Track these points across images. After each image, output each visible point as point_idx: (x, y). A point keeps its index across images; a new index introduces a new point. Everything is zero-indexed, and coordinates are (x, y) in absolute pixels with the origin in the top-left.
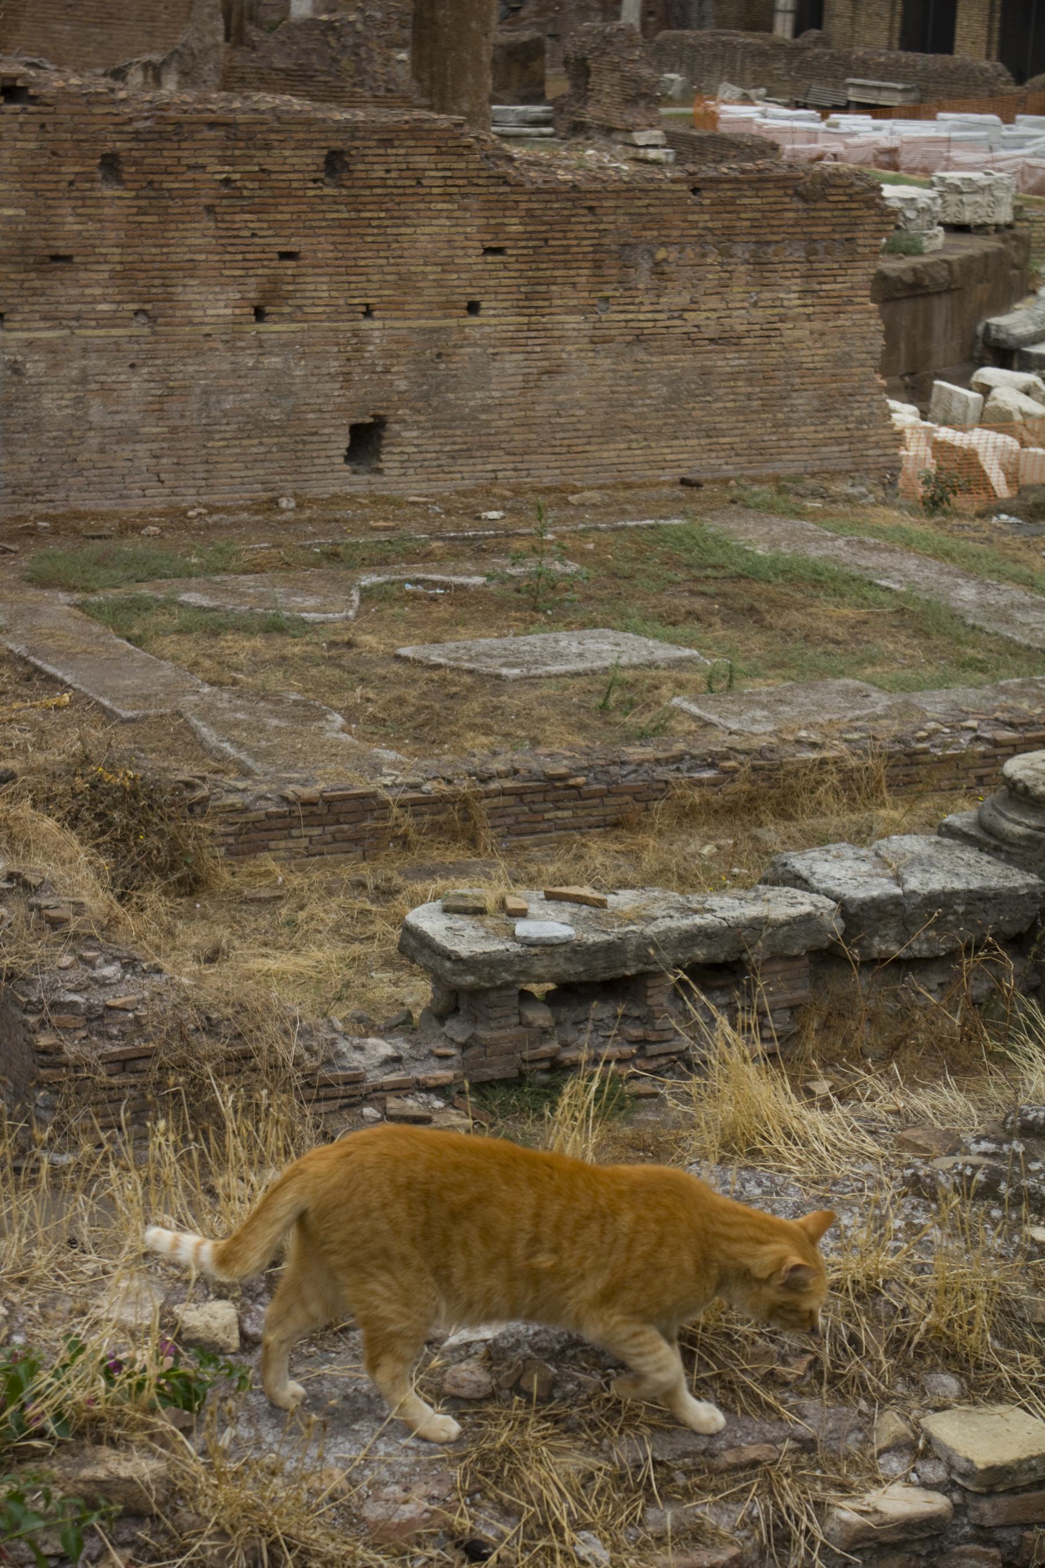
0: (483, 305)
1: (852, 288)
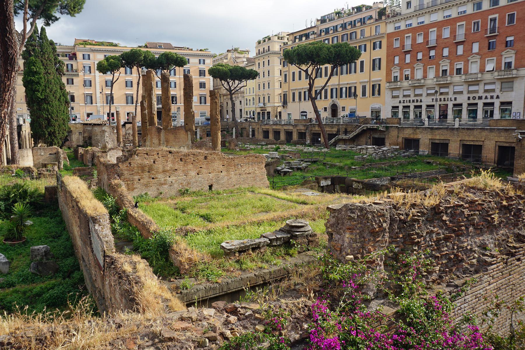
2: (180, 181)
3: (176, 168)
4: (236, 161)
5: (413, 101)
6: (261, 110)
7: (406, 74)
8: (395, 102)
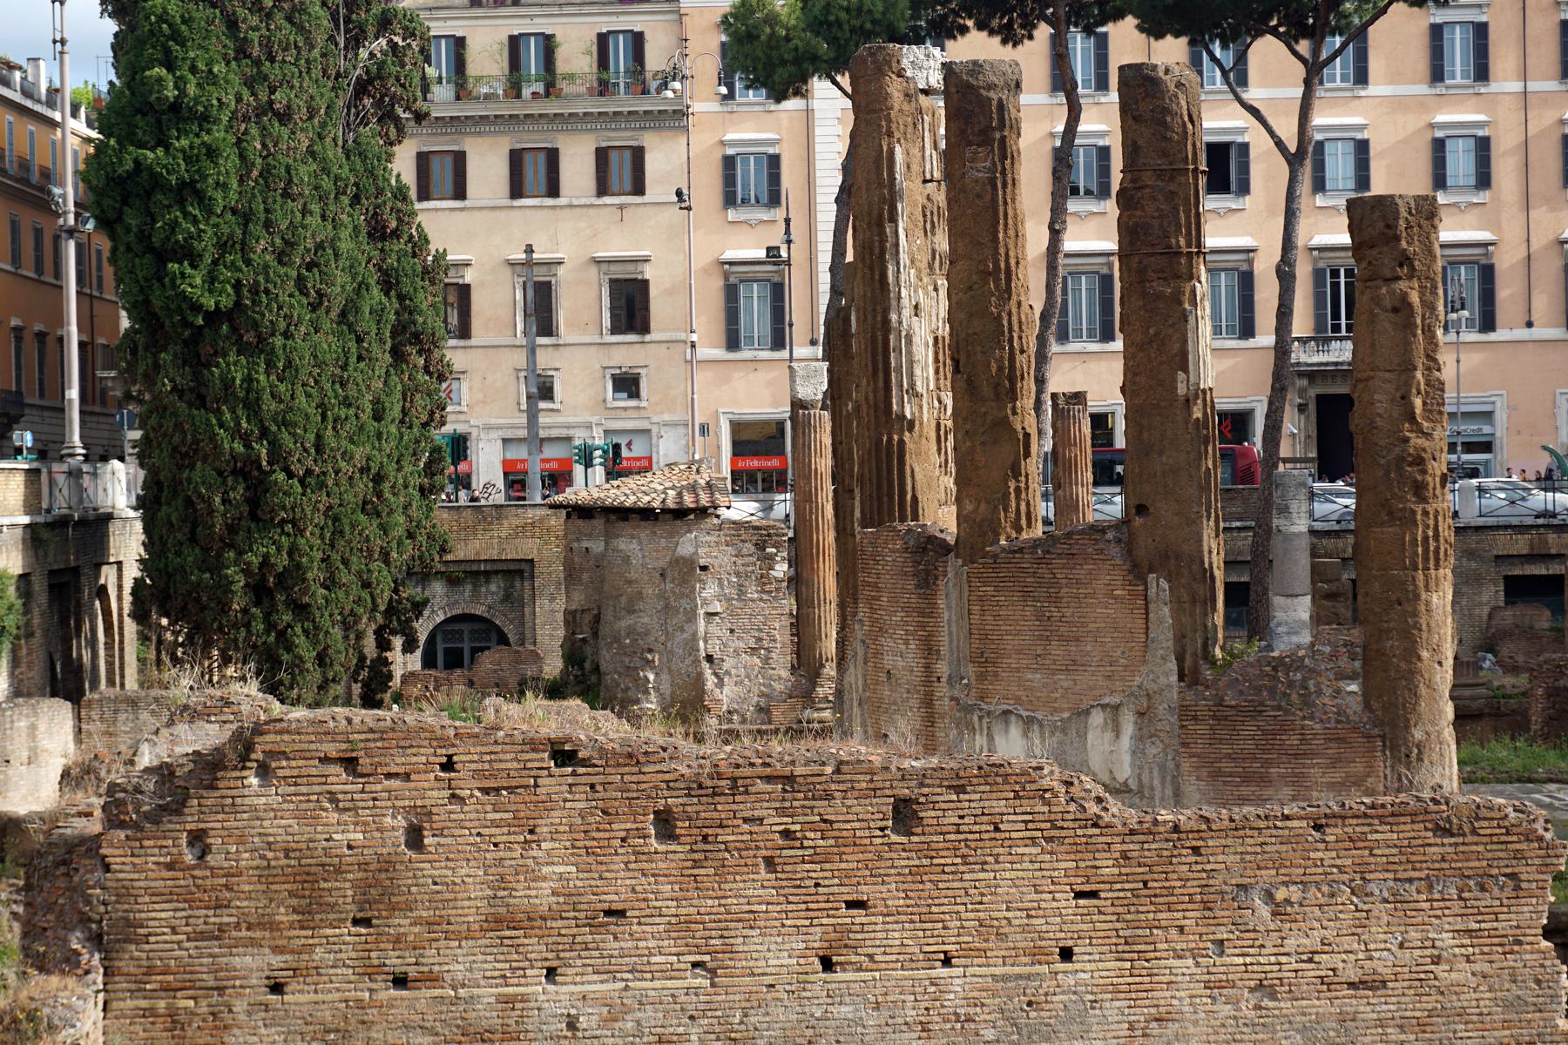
0: (1076, 950)
1: (1518, 927)
2: (649, 1015)
3: (613, 900)
4: (1224, 859)
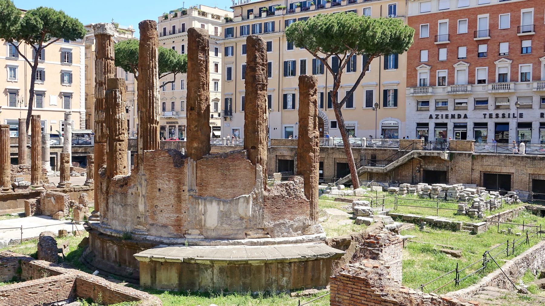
5: (453, 116)
6: (168, 123)
7: (422, 78)
8: (423, 117)
